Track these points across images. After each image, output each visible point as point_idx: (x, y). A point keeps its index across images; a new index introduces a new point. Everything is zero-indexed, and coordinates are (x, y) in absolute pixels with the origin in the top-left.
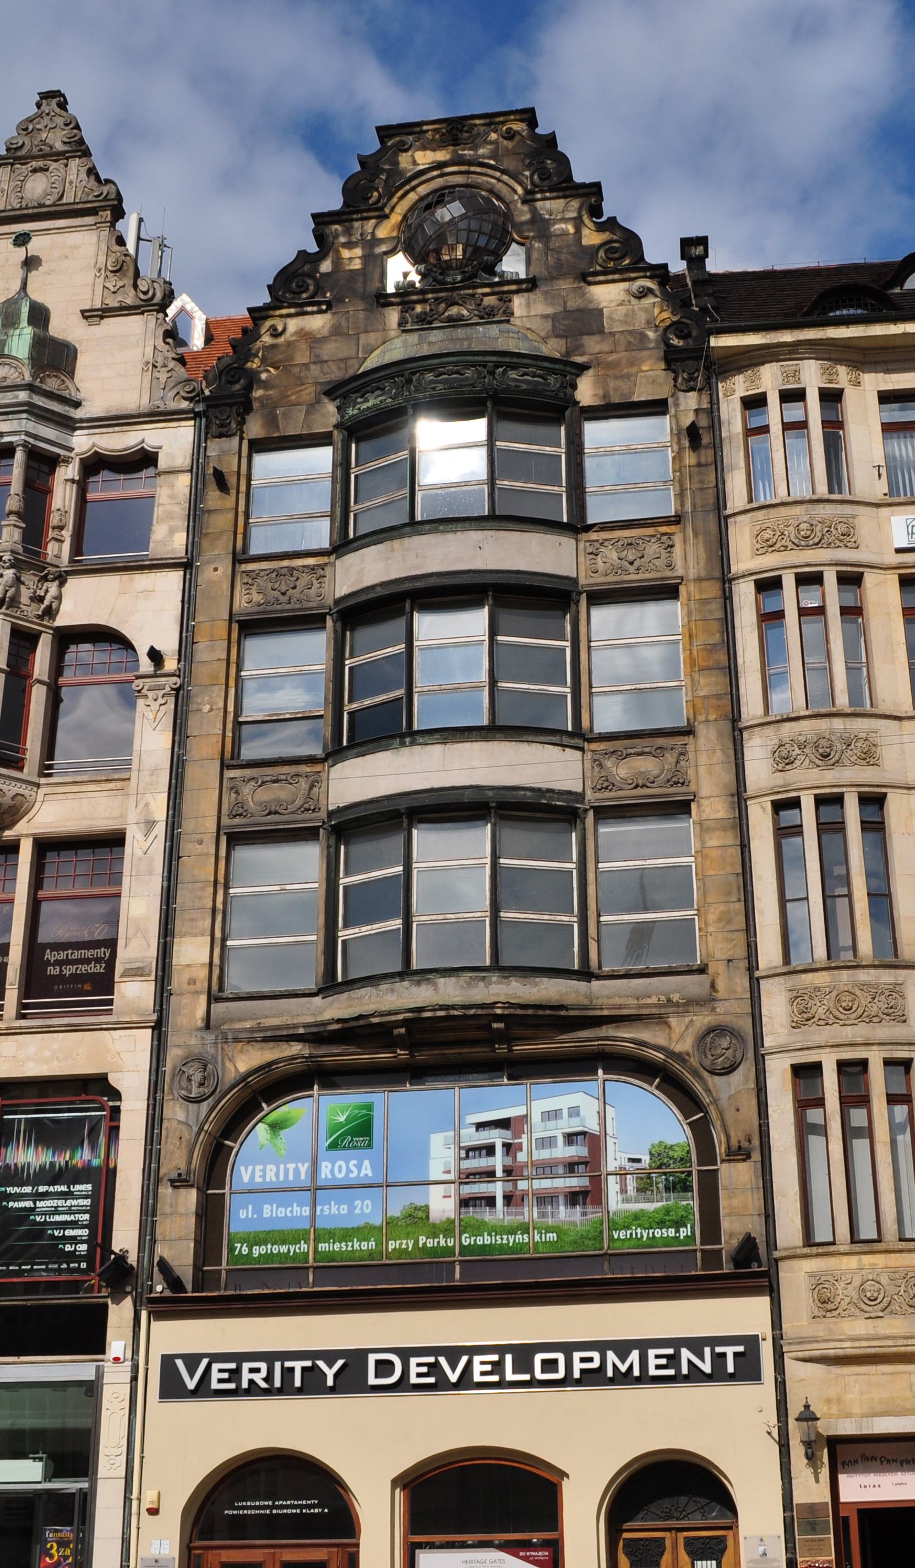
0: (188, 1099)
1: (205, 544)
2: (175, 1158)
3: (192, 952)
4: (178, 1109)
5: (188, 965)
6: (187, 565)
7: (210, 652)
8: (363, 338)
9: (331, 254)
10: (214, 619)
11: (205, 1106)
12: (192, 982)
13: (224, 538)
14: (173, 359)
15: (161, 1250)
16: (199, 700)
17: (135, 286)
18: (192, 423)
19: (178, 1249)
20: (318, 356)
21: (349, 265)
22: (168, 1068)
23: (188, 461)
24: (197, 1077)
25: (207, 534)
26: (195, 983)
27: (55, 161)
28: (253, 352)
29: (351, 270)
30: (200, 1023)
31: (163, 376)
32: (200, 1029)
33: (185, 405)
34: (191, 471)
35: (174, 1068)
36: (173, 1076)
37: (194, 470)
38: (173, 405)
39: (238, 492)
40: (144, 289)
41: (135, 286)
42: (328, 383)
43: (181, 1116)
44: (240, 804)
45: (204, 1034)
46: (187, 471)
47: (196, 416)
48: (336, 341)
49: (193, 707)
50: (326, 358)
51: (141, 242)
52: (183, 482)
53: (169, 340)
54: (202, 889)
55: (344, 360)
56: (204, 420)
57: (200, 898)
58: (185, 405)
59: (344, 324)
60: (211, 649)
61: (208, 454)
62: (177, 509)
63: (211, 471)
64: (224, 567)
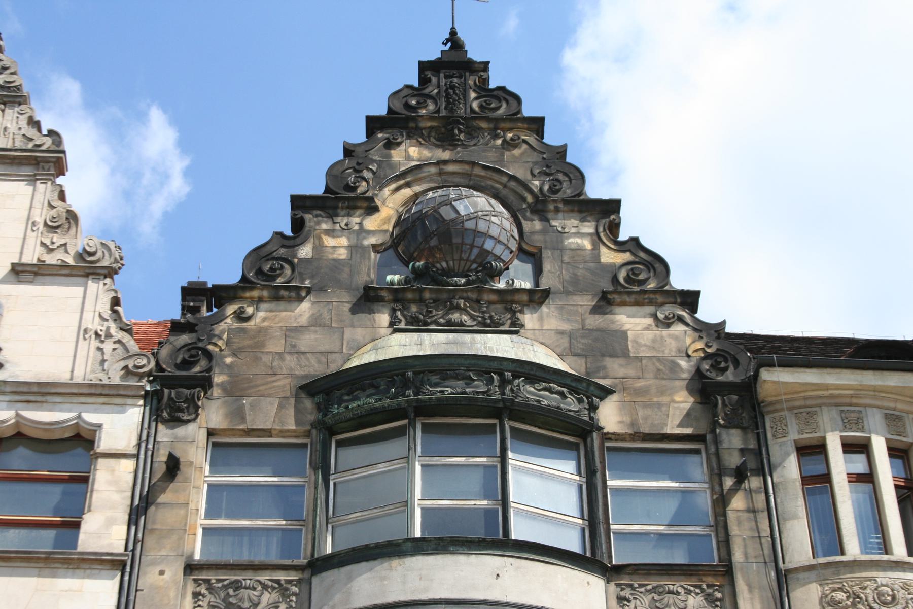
8: (348, 333)
9: (312, 240)
20: (294, 346)
21: (333, 254)
28: (217, 332)
29: (334, 260)
34: (137, 456)
37: (142, 456)
42: (306, 376)
48: (316, 332)
50: (303, 349)
55: (327, 353)
59: (326, 316)
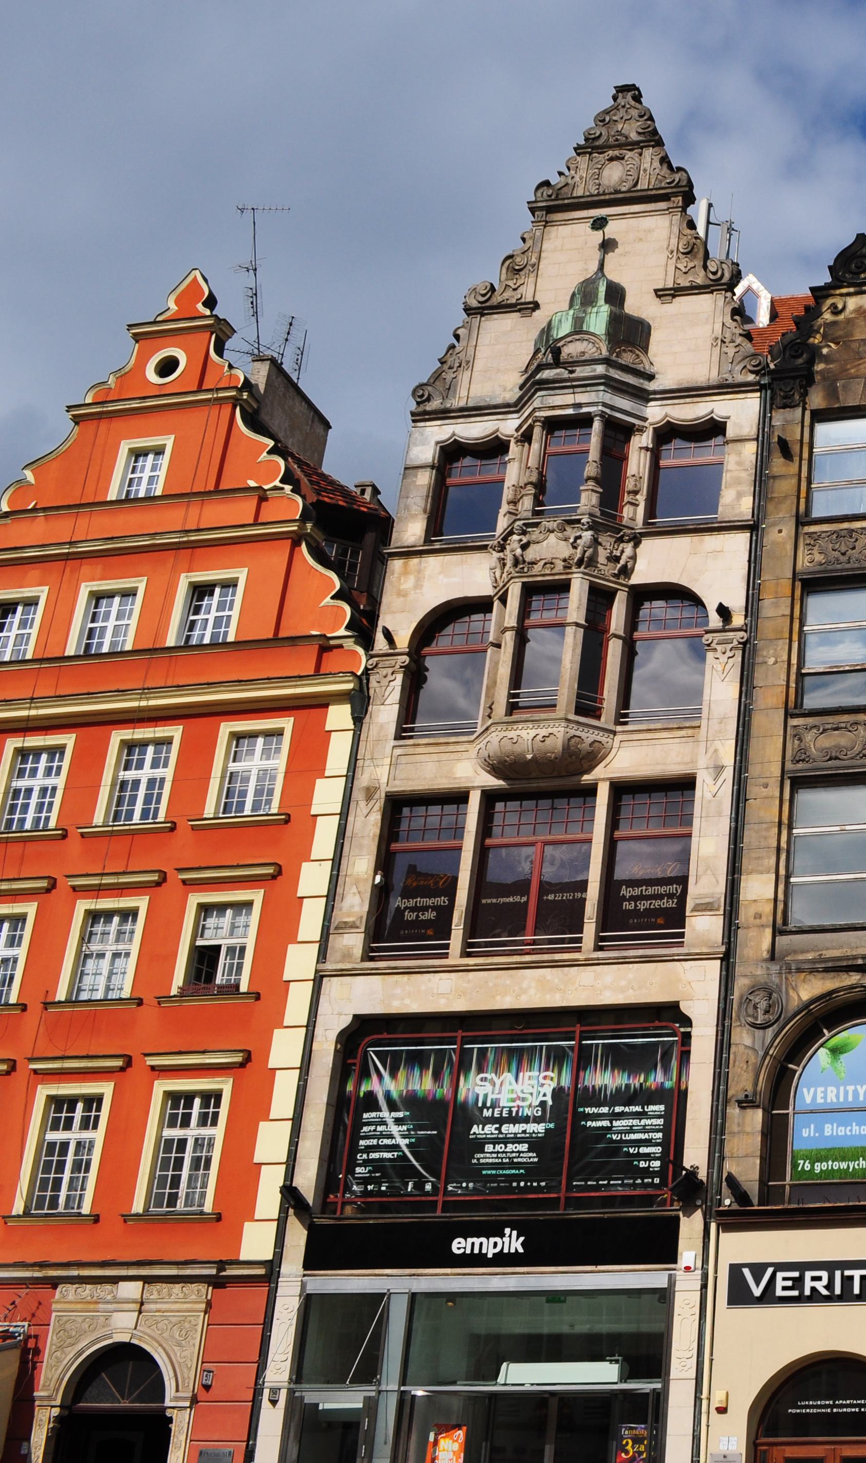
0: (754, 1026)
1: (770, 507)
2: (742, 1081)
3: (758, 889)
4: (745, 1035)
5: (755, 901)
6: (753, 527)
7: (775, 609)
10: (778, 577)
11: (770, 1032)
12: (758, 916)
13: (788, 502)
14: (740, 335)
15: (729, 1167)
16: (765, 653)
17: (705, 267)
18: (758, 394)
19: (745, 1166)
22: (736, 996)
23: (755, 430)
24: (763, 1005)
25: (772, 498)
26: (760, 917)
27: (630, 150)
30: (765, 955)
31: (731, 351)
32: (765, 960)
33: (751, 378)
34: (757, 439)
35: (741, 997)
36: (740, 1004)
37: (760, 438)
38: (740, 378)
39: (801, 459)
40: (714, 270)
41: (705, 267)
43: (748, 1041)
44: (803, 750)
45: (769, 965)
46: (753, 440)
47: (762, 388)
49: (759, 660)
51: (710, 226)
52: (750, 450)
53: (737, 318)
54: (767, 829)
56: (769, 392)
57: (765, 838)
58: (751, 378)
60: (776, 605)
61: (773, 424)
62: (744, 475)
63: (776, 439)
64: (788, 529)
